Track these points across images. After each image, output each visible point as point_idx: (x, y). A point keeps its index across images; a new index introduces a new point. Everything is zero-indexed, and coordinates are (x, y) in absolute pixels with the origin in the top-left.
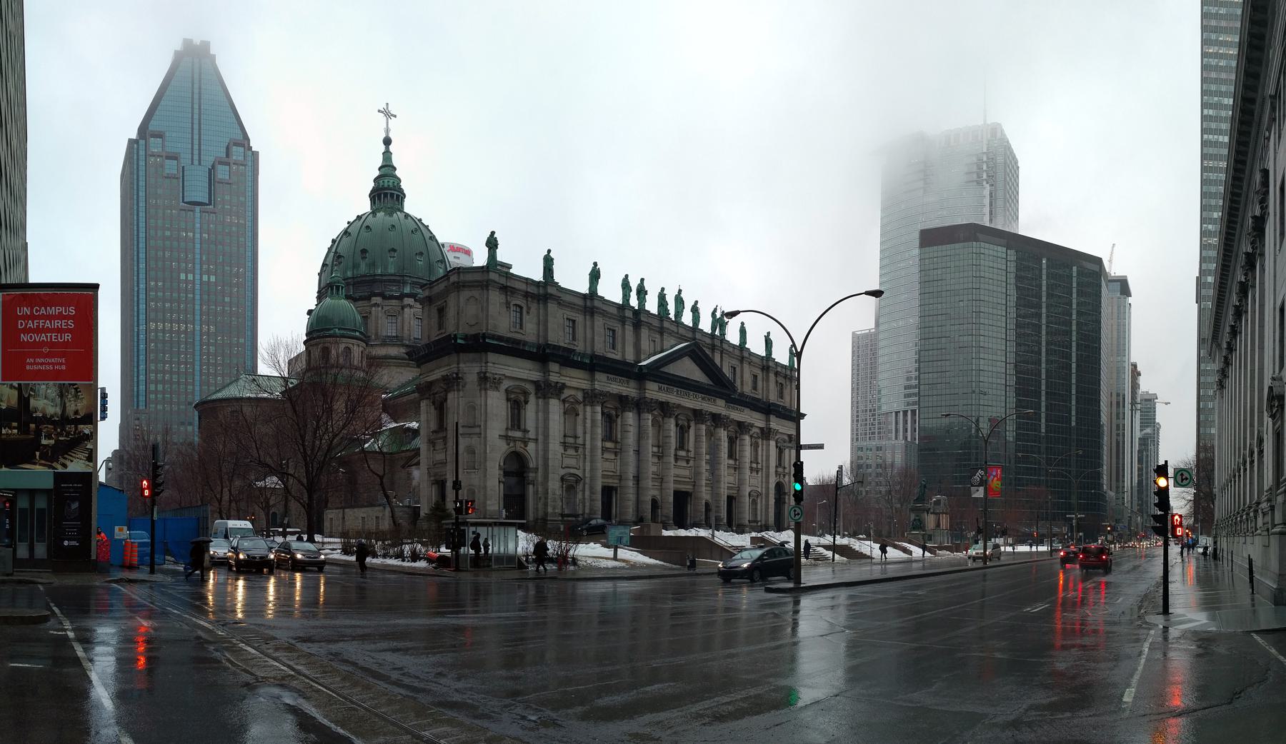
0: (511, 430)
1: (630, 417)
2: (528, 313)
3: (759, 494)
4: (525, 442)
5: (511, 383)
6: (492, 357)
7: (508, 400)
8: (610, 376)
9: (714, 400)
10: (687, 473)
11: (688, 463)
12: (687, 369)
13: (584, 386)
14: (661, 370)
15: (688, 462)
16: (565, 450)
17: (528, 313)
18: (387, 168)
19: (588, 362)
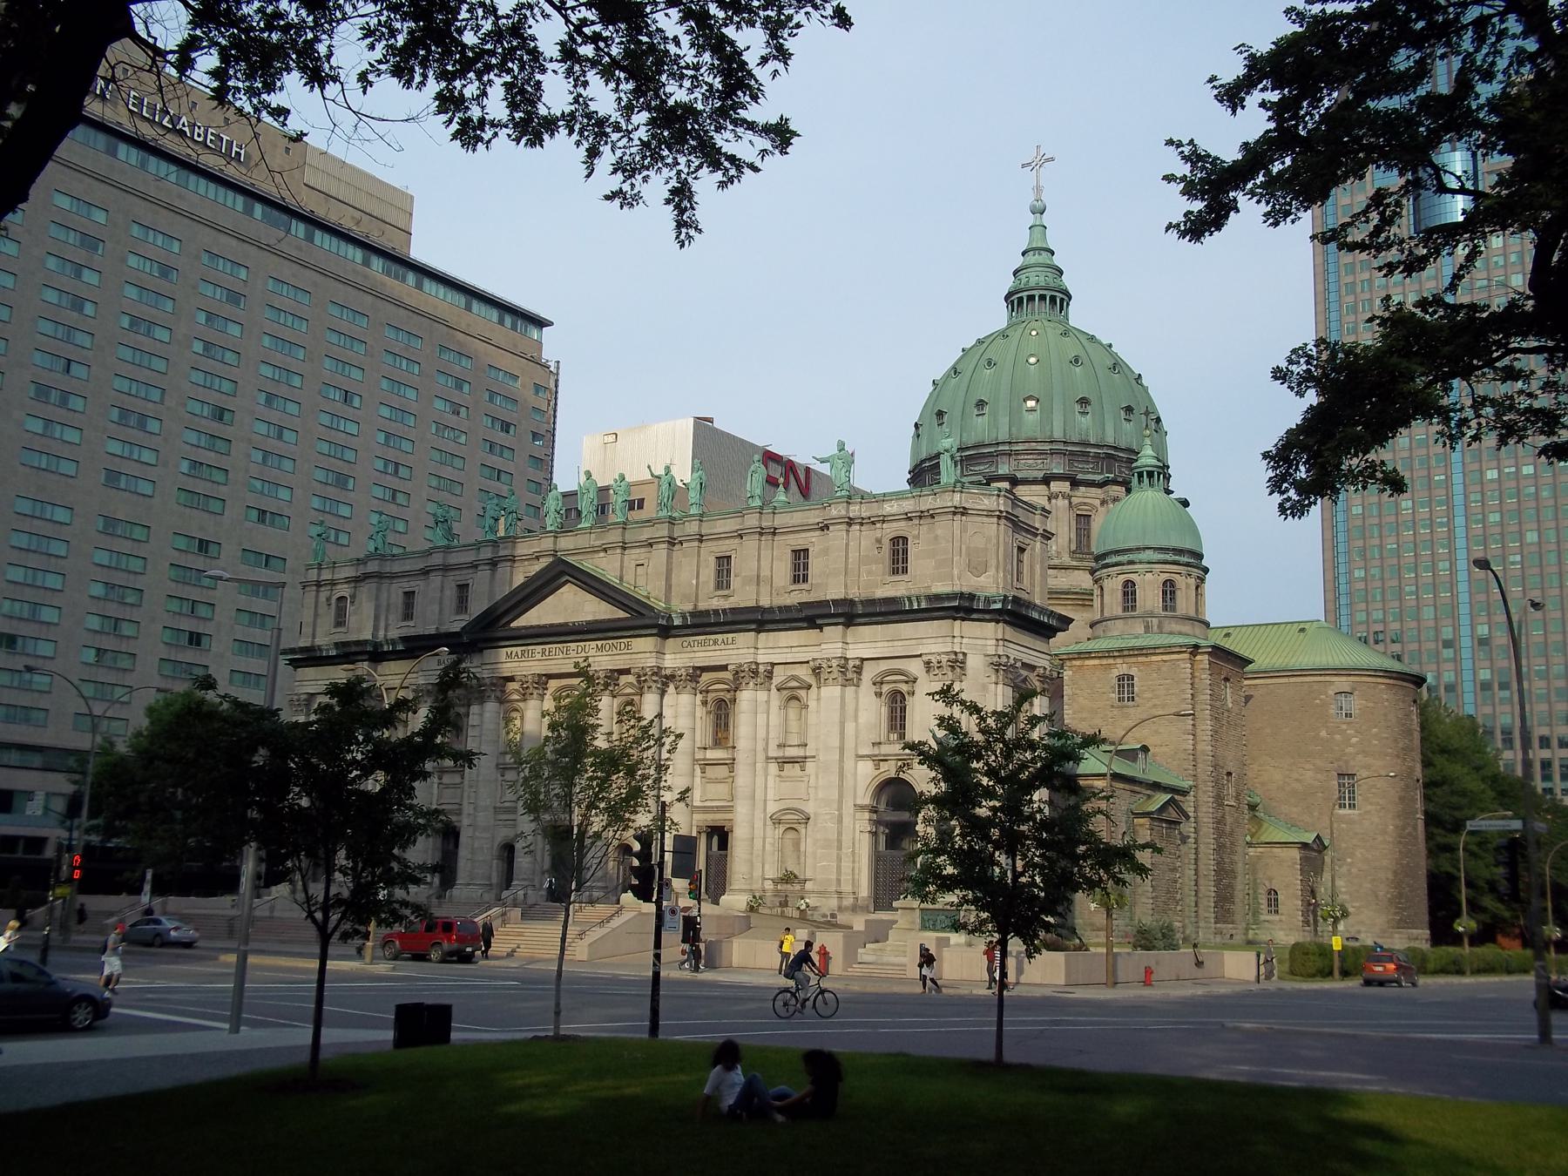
2: (352, 603)
9: (628, 646)
12: (569, 605)
18: (1039, 249)
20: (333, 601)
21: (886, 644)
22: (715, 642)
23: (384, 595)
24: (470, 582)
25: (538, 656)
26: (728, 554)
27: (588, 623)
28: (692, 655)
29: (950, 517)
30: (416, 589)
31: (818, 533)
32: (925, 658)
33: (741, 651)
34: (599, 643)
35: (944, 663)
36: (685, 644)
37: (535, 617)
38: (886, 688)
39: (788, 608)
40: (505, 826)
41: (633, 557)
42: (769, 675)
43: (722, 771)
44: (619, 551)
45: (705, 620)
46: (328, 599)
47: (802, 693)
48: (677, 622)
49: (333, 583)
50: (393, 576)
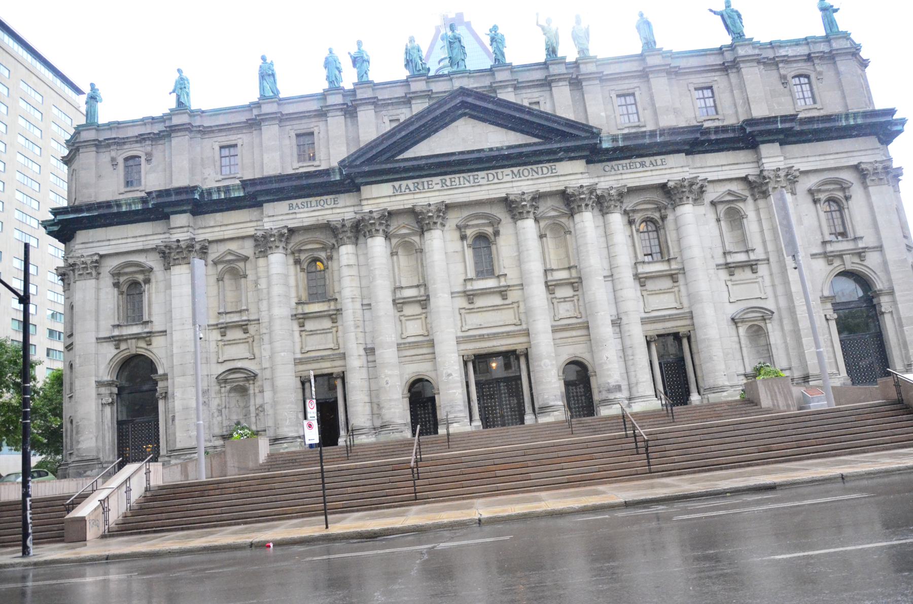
0: (118, 326)
1: (346, 252)
2: (148, 161)
3: (766, 315)
4: (147, 337)
5: (114, 263)
6: (82, 236)
7: (116, 285)
8: (294, 202)
10: (507, 316)
11: (504, 297)
13: (251, 232)
14: (400, 157)
15: (502, 293)
16: (223, 335)
17: (148, 161)
19: (242, 194)
20: (120, 161)
21: (818, 158)
22: (643, 165)
23: (198, 149)
24: (316, 130)
25: (438, 187)
26: (631, 91)
27: (509, 147)
28: (620, 177)
29: (850, 57)
30: (239, 143)
31: (718, 73)
32: (863, 166)
33: (674, 170)
34: (515, 170)
35: (879, 171)
36: (607, 169)
37: (423, 149)
38: (823, 196)
39: (724, 129)
40: (412, 362)
41: (525, 96)
42: (702, 190)
43: (667, 283)
44: (510, 89)
45: (640, 142)
46: (113, 159)
47: (741, 205)
48: (605, 145)
49: (120, 143)
50: (205, 131)
